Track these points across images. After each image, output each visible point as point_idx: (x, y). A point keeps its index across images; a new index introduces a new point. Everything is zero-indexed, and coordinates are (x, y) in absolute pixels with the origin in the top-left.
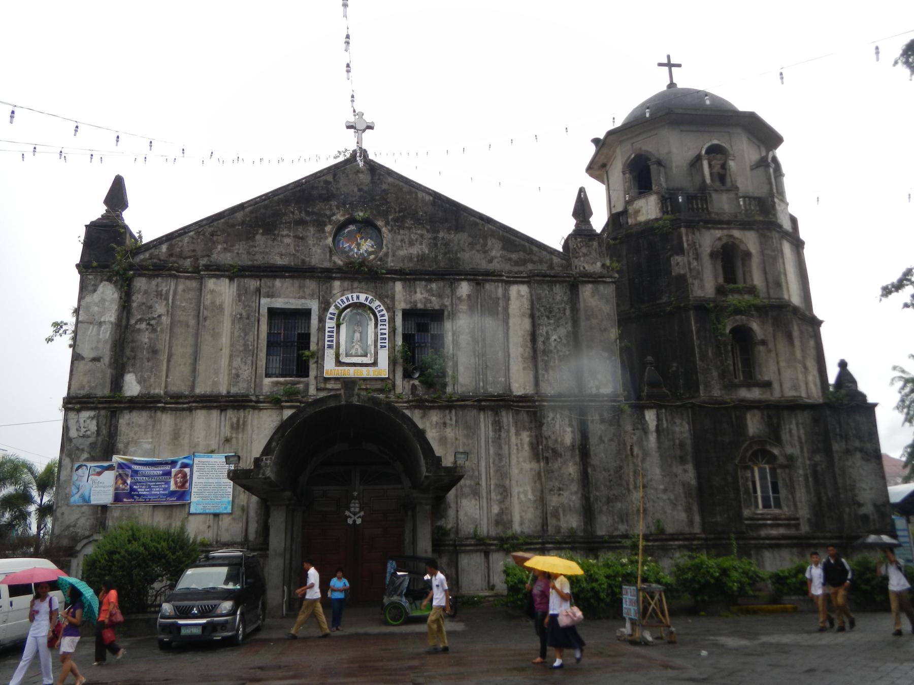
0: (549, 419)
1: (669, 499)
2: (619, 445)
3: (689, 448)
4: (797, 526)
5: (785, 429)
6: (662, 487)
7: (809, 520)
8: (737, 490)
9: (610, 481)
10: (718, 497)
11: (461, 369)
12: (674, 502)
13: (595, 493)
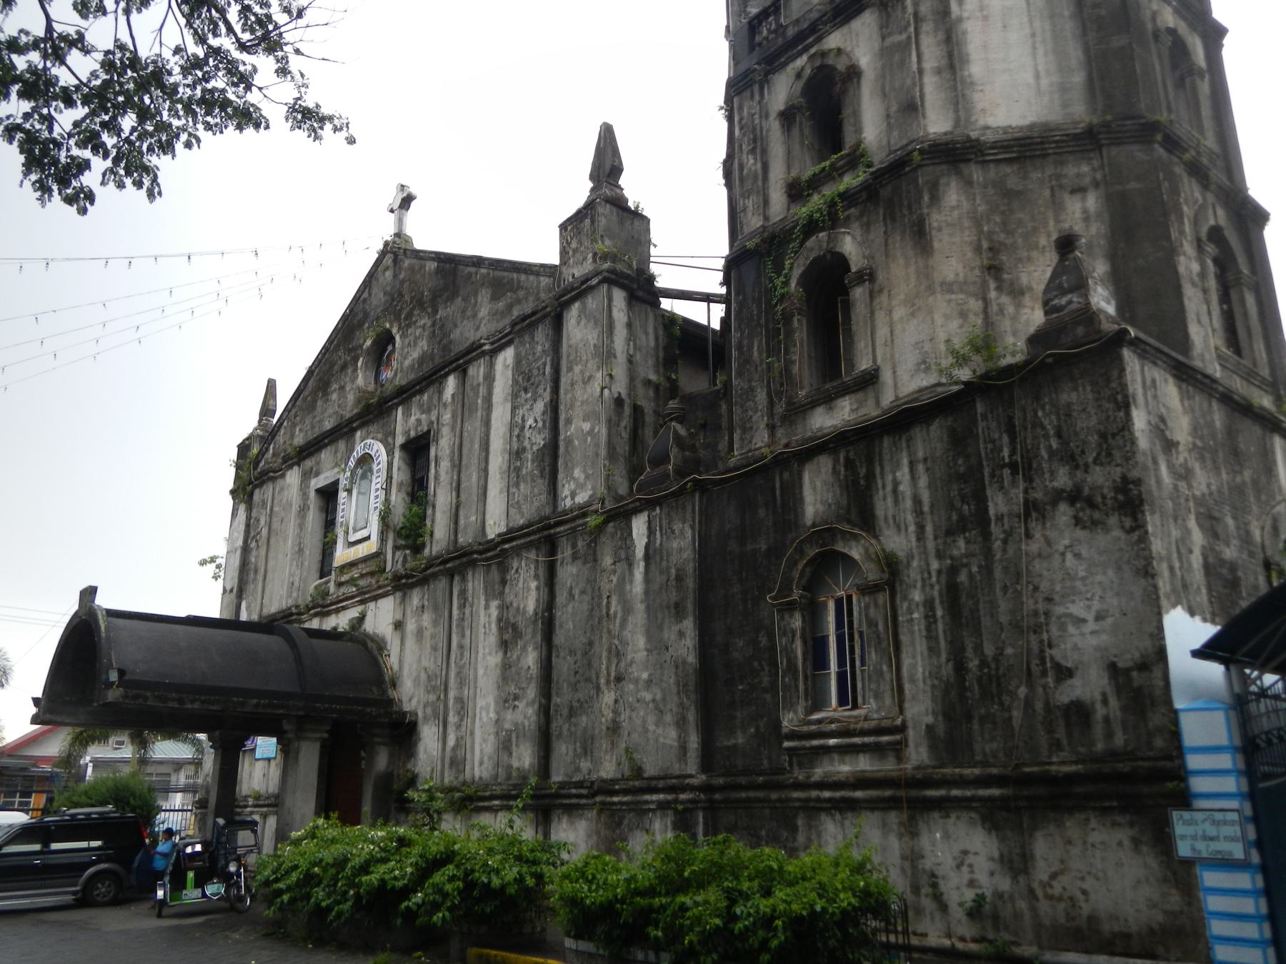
0: (513, 571)
1: (654, 700)
2: (593, 599)
3: (690, 583)
4: (898, 749)
5: (884, 487)
6: (645, 676)
7: (930, 729)
8: (774, 664)
9: (576, 673)
10: (740, 687)
11: (438, 515)
12: (661, 705)
13: (556, 700)
